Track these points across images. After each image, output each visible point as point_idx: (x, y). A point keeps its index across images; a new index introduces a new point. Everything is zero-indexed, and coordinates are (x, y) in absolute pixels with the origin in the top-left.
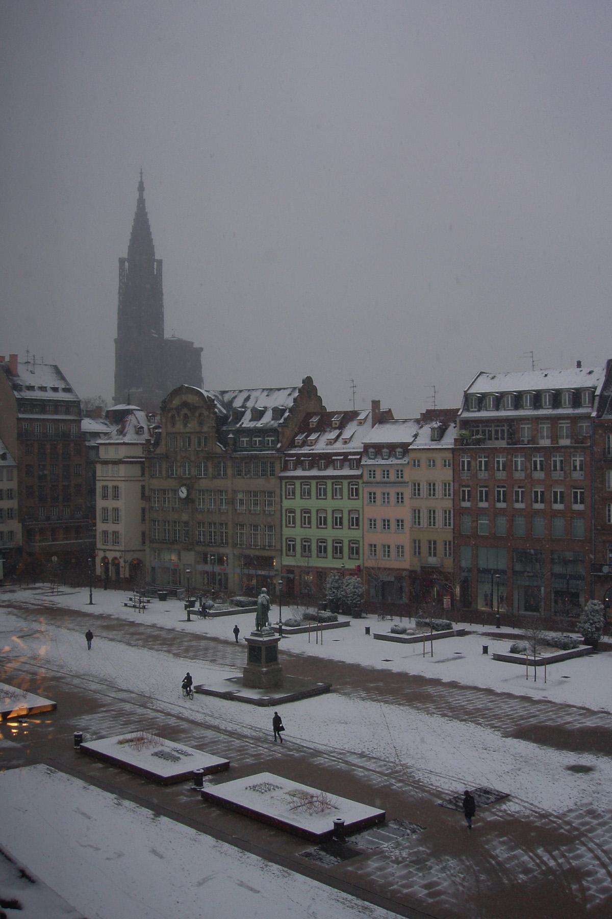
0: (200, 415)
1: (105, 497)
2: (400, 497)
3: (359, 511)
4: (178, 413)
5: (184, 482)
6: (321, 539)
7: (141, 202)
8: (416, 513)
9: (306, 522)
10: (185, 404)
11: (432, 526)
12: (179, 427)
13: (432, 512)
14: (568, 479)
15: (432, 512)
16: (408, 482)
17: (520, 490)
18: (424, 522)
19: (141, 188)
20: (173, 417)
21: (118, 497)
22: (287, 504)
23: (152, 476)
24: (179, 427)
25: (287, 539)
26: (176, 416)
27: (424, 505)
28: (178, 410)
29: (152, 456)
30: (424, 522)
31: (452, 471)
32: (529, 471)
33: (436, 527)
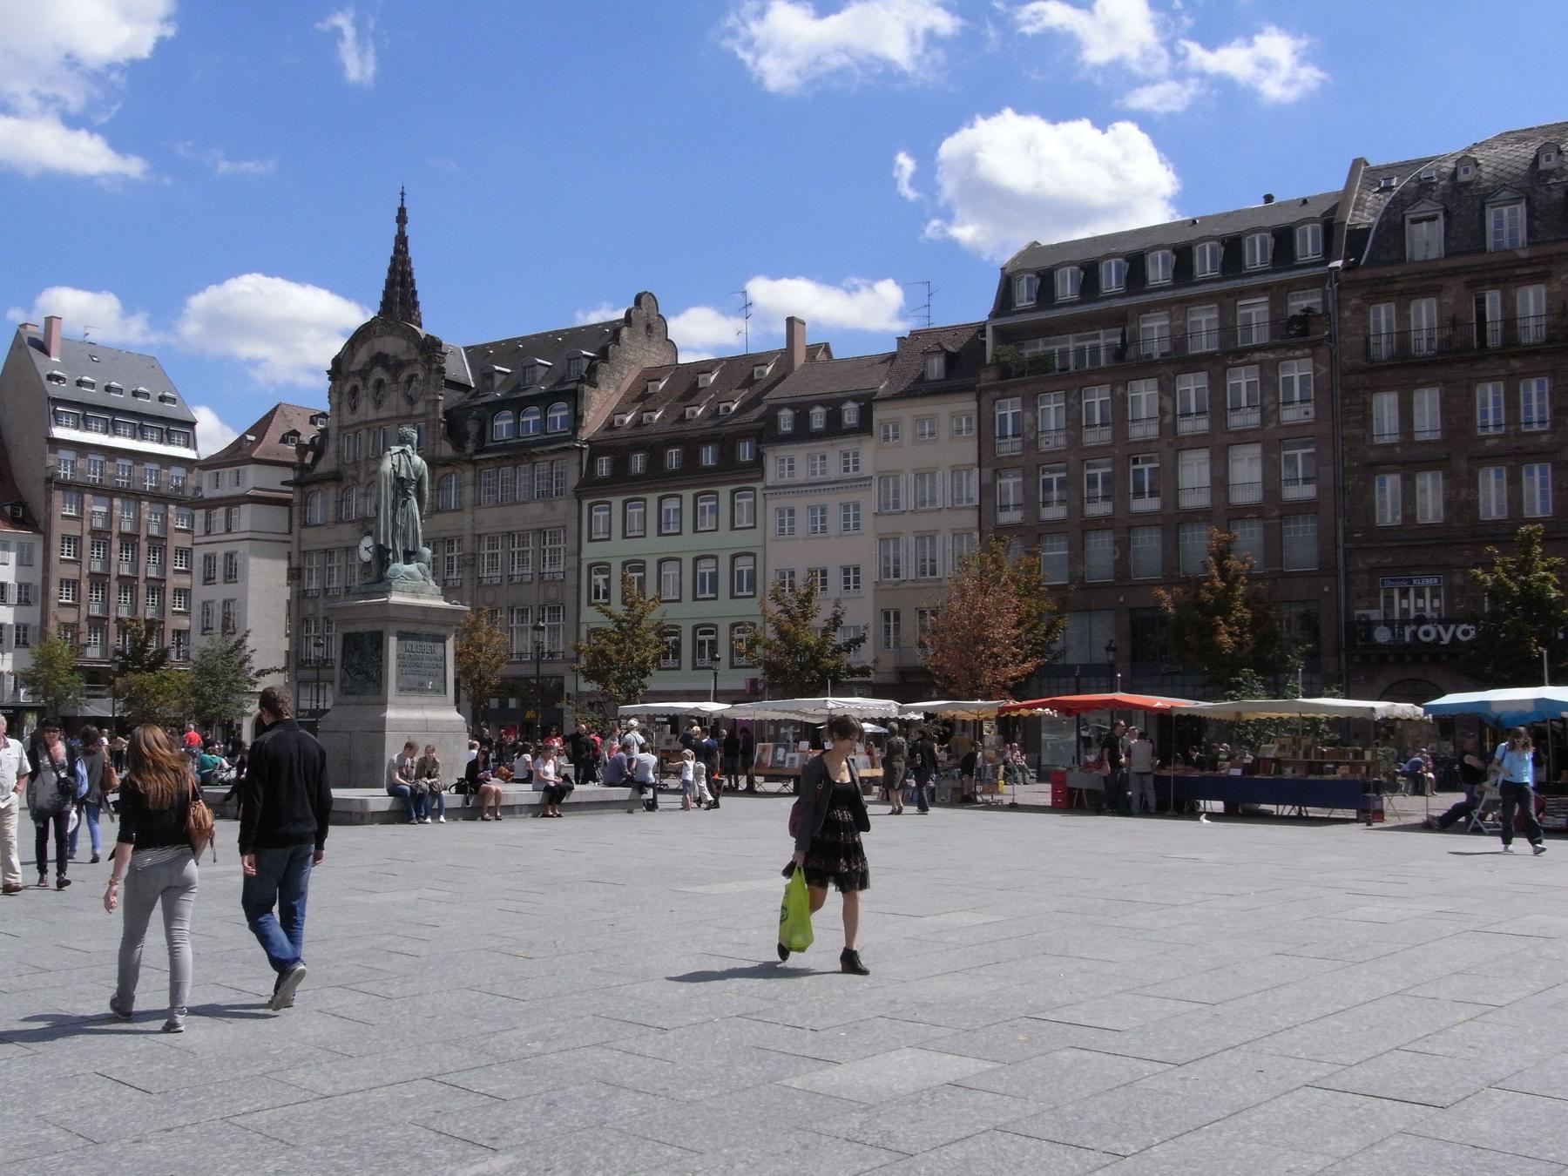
0: (411, 378)
1: (210, 579)
3: (754, 555)
4: (365, 379)
7: (401, 241)
10: (380, 359)
11: (928, 576)
12: (367, 409)
14: (1272, 425)
17: (1146, 467)
19: (402, 218)
20: (355, 390)
21: (235, 576)
23: (305, 525)
24: (367, 409)
26: (361, 387)
28: (364, 374)
29: (308, 476)
31: (976, 442)
32: (1168, 419)
33: (938, 577)
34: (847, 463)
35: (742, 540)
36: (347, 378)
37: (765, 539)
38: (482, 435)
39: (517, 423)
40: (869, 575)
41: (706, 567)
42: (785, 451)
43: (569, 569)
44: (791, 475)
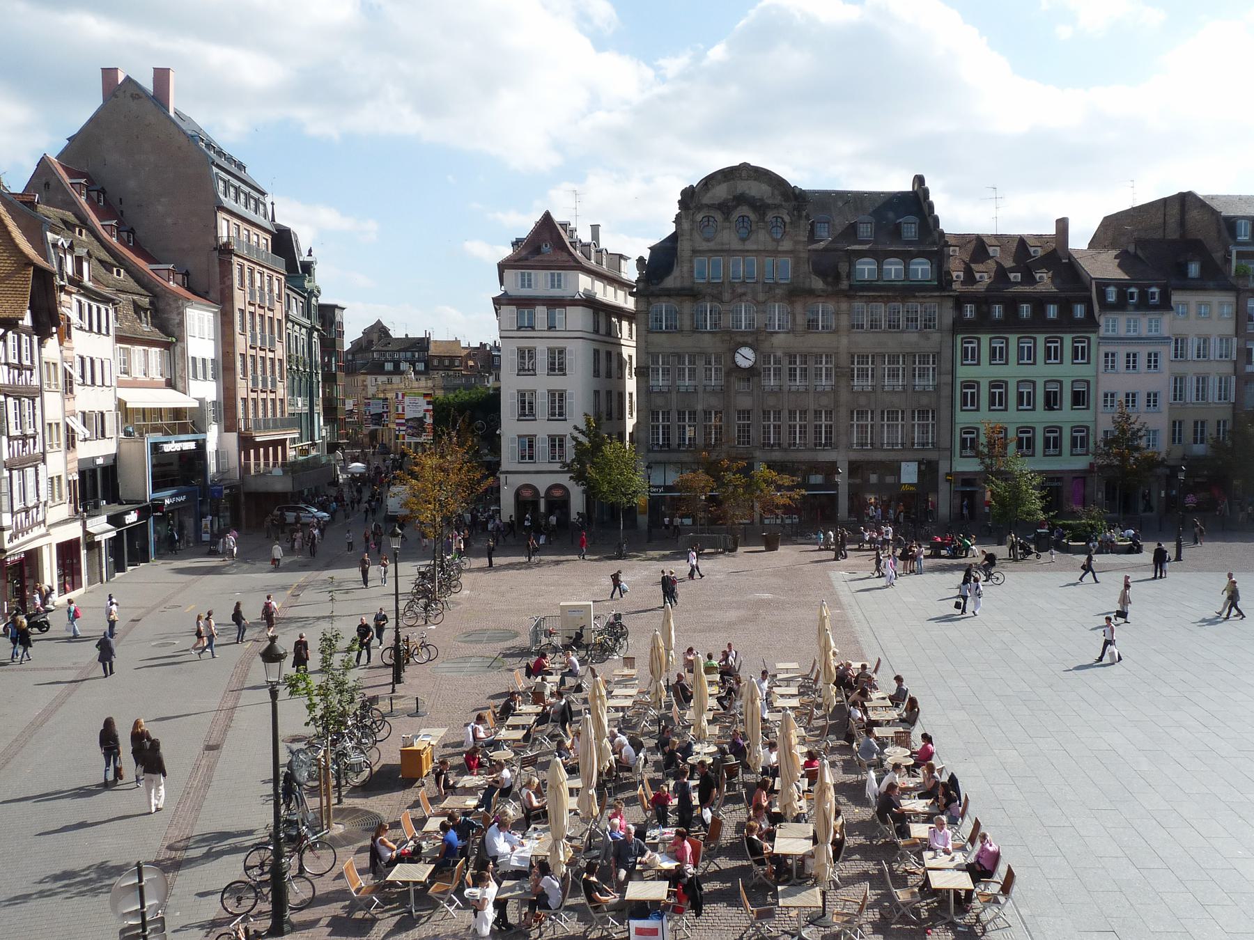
2: (1153, 361)
3: (1088, 382)
5: (740, 339)
6: (1022, 427)
8: (1179, 381)
9: (998, 400)
10: (741, 199)
11: (1200, 401)
13: (1202, 380)
15: (1202, 380)
16: (1168, 338)
18: (1190, 394)
22: (965, 372)
25: (961, 429)
27: (1191, 370)
28: (725, 208)
30: (1190, 394)
31: (1234, 321)
34: (1129, 326)
35: (1083, 371)
36: (700, 208)
37: (1097, 372)
38: (849, 276)
39: (880, 269)
40: (1166, 398)
41: (1053, 388)
42: (1111, 315)
43: (944, 384)
44: (1113, 330)
